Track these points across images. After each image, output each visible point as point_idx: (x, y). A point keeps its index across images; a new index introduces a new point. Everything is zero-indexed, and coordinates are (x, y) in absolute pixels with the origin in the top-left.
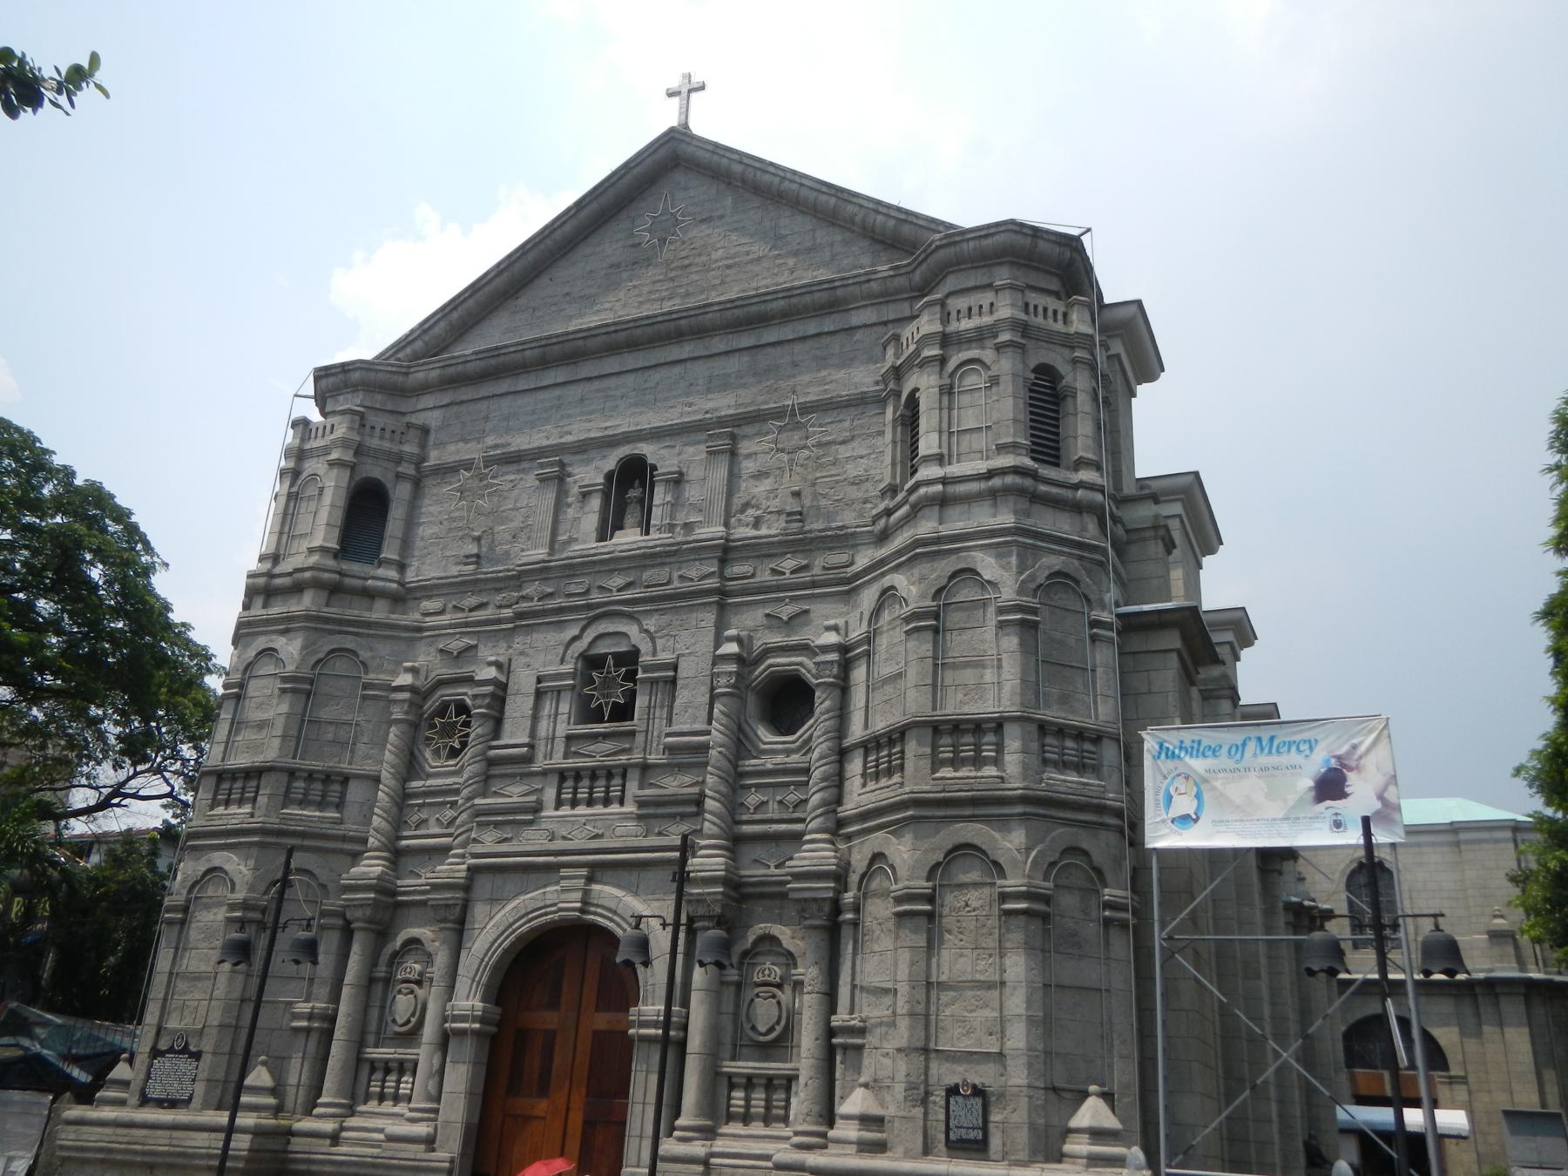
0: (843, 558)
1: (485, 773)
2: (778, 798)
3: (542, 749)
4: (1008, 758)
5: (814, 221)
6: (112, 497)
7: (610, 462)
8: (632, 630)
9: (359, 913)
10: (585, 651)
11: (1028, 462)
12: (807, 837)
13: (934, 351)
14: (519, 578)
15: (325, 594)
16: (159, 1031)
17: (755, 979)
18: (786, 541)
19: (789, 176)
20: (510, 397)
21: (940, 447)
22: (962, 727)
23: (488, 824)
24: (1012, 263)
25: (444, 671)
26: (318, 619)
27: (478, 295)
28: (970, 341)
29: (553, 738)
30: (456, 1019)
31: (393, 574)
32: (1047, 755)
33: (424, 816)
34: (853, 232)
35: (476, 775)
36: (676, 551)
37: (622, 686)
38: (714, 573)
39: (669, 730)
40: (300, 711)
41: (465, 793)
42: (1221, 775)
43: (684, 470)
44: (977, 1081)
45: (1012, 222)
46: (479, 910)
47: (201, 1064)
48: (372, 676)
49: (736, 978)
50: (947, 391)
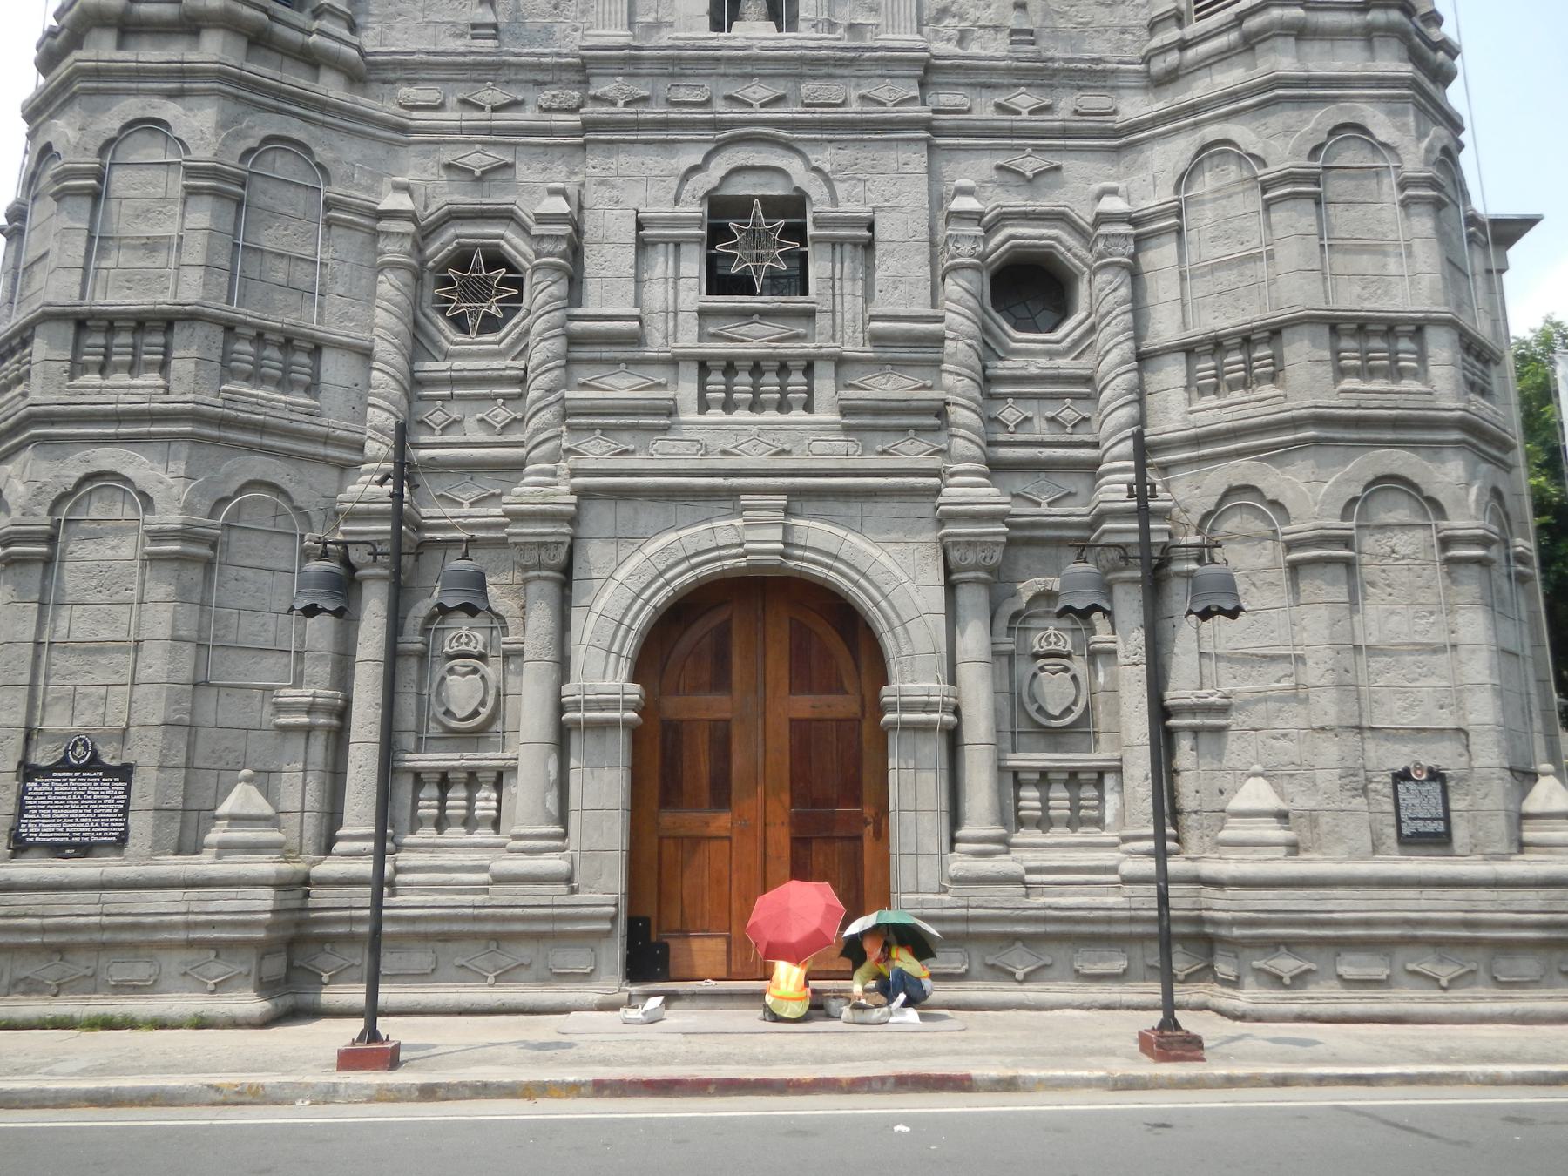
2: (1049, 414)
3: (660, 326)
4: (1434, 371)
8: (794, 165)
10: (715, 189)
14: (583, 69)
15: (242, 44)
18: (1018, 69)
22: (1371, 327)
25: (456, 198)
26: (241, 81)
29: (676, 313)
31: (343, 32)
33: (455, 416)
36: (853, 60)
37: (781, 245)
38: (915, 98)
40: (230, 229)
41: (543, 381)
46: (595, 555)
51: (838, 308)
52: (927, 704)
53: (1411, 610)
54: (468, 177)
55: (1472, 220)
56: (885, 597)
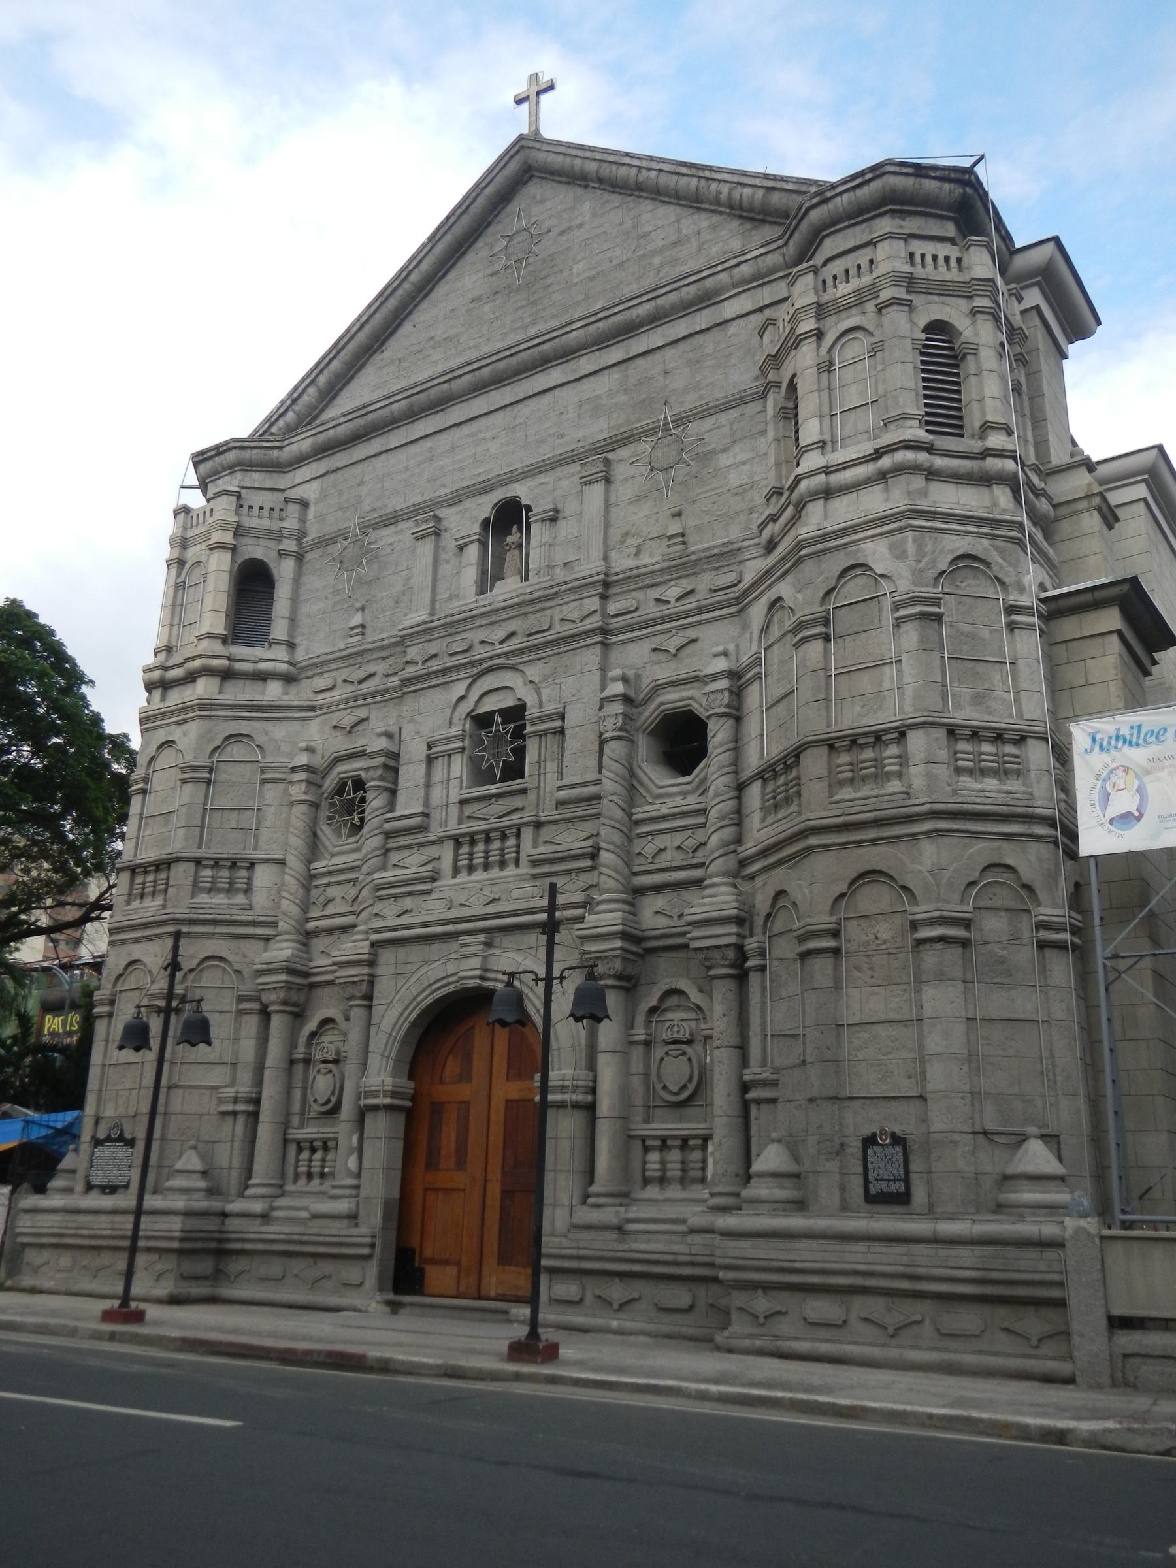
0: (731, 578)
1: (383, 847)
5: (678, 209)
6: (31, 615)
7: (484, 507)
9: (273, 997)
10: (473, 711)
11: (920, 434)
12: (707, 882)
13: (808, 325)
16: (97, 1121)
17: (664, 1037)
19: (645, 164)
20: (383, 456)
21: (821, 433)
22: (860, 741)
23: (388, 897)
24: (893, 212)
26: (212, 706)
27: (343, 353)
28: (849, 307)
29: (447, 806)
30: (368, 1094)
31: (281, 653)
32: (960, 763)
34: (721, 213)
35: (376, 849)
36: (556, 593)
37: (512, 743)
39: (560, 783)
40: (201, 800)
42: (1167, 763)
43: (560, 507)
44: (897, 1129)
45: (890, 162)
47: (135, 1150)
48: (269, 759)
49: (644, 1037)
50: (827, 367)
51: (542, 784)
52: (563, 1087)
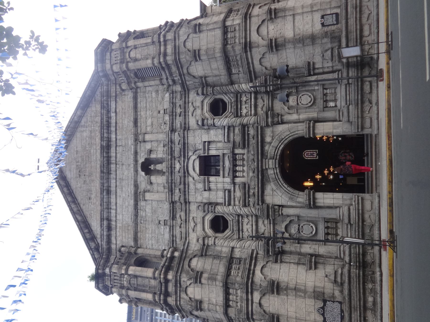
8: (193, 158)
10: (198, 175)
24: (106, 52)
29: (224, 182)
38: (179, 133)
45: (95, 50)
53: (286, 24)
54: (196, 226)
55: (202, 16)
56: (285, 137)
